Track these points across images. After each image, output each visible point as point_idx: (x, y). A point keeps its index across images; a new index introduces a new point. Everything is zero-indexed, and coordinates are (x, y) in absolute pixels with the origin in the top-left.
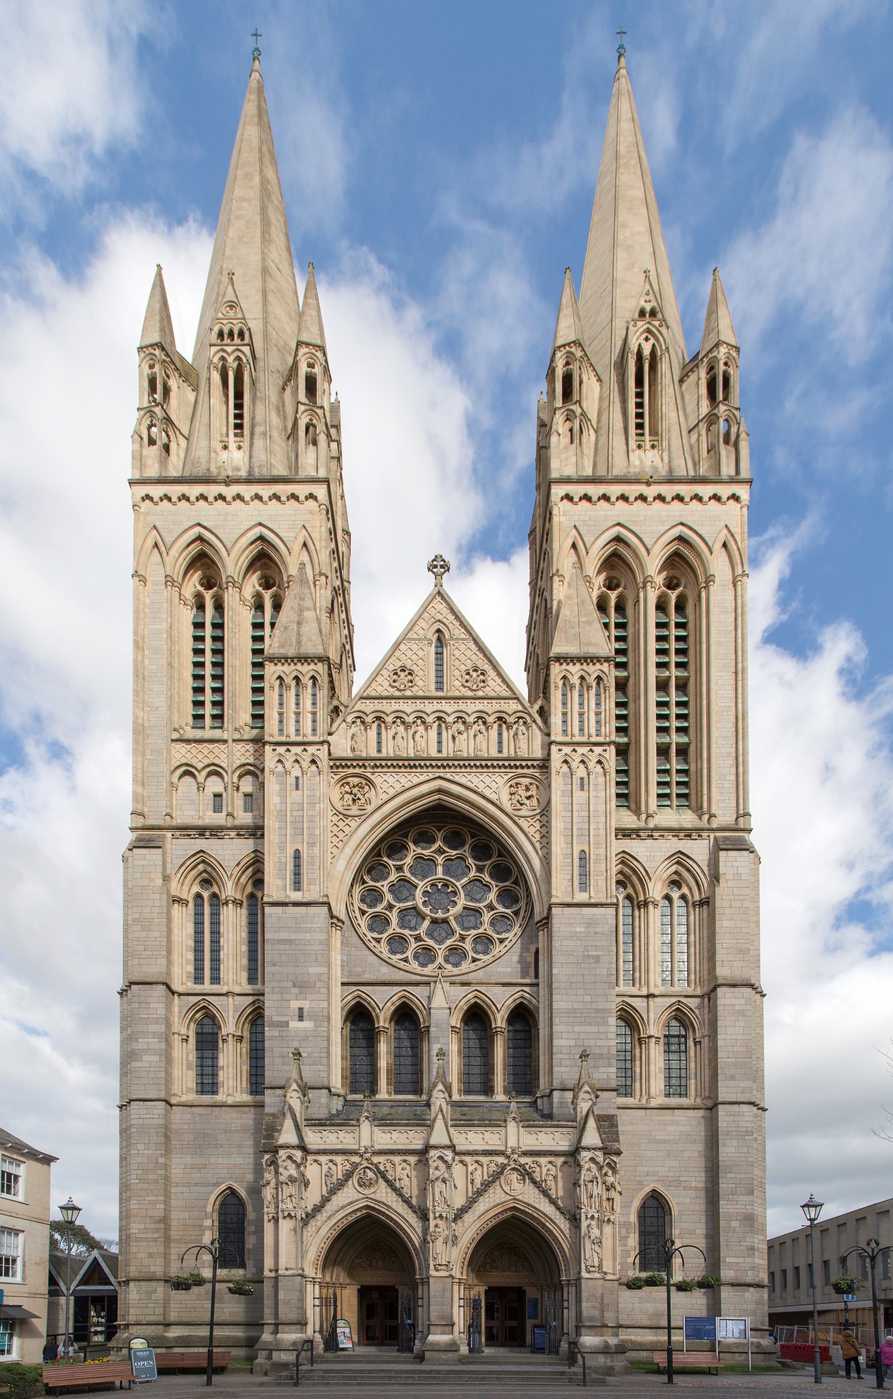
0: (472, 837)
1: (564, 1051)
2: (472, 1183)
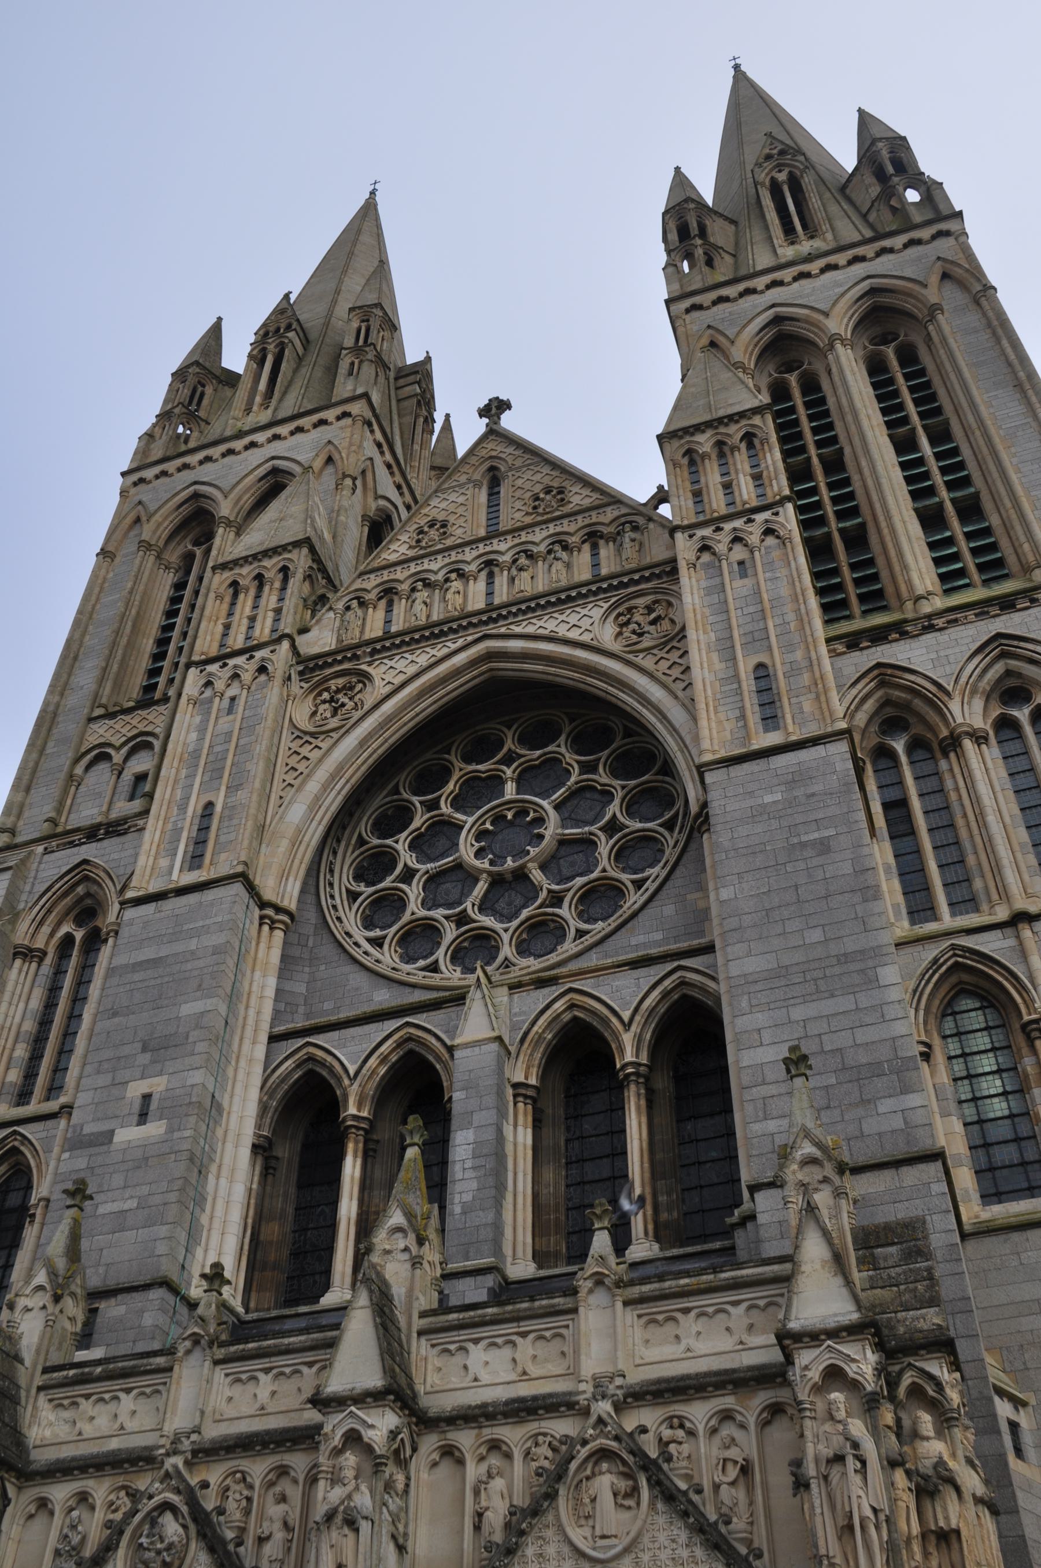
0: (572, 721)
1: (770, 1076)
2: (477, 1528)
